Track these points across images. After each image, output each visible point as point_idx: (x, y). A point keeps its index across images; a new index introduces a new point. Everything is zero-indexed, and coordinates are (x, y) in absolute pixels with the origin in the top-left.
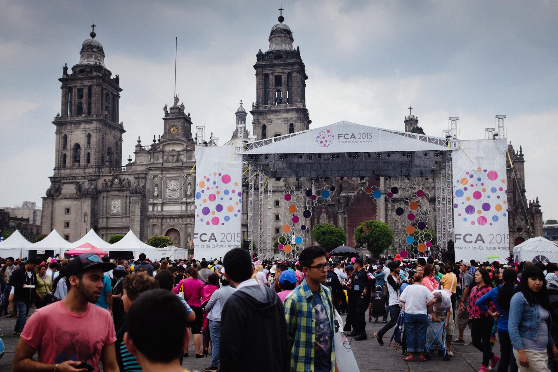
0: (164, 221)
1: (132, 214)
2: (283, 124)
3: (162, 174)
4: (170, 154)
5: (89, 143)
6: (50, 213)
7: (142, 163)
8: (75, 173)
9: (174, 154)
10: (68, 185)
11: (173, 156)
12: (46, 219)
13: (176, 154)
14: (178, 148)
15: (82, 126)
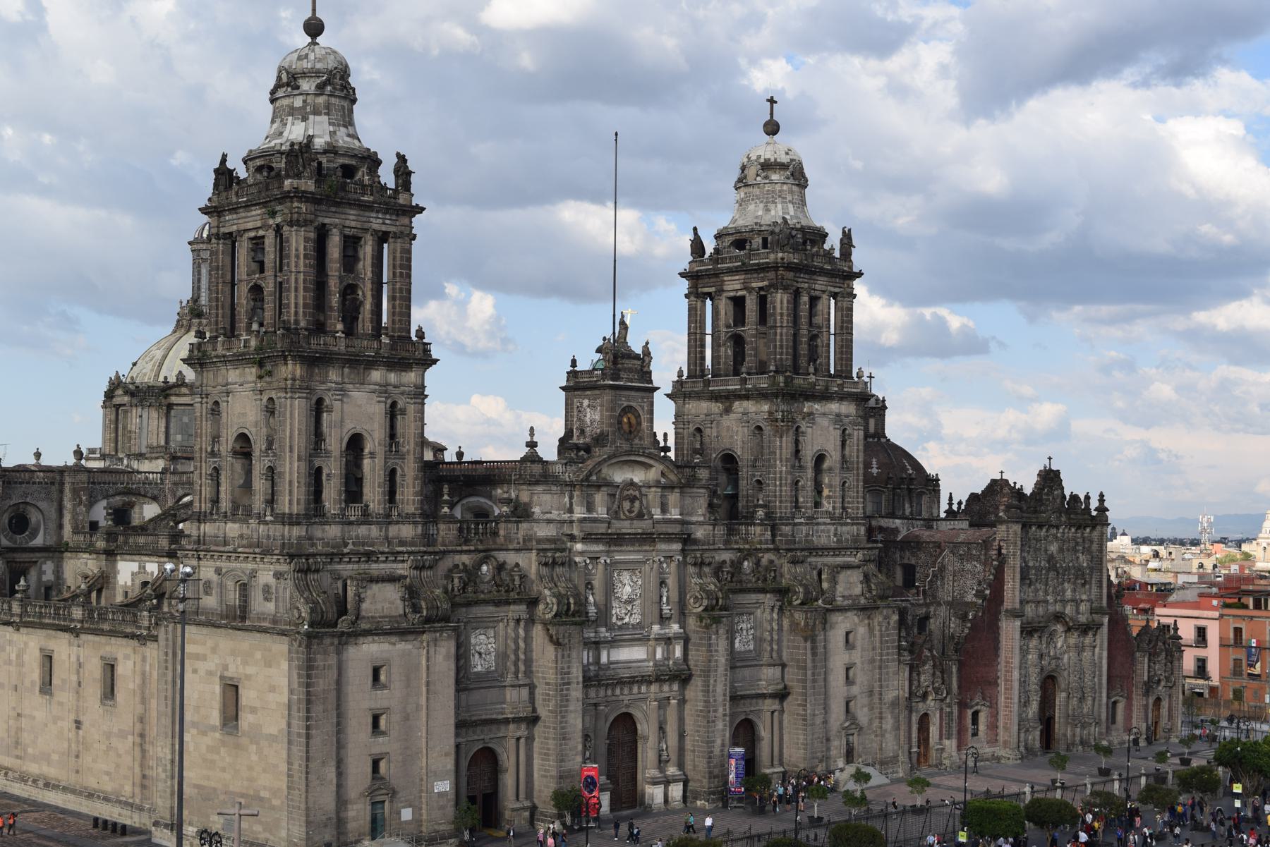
0: (609, 692)
1: (563, 679)
2: (831, 428)
3: (608, 553)
4: (626, 493)
5: (392, 436)
6: (333, 687)
7: (548, 516)
8: (357, 537)
9: (634, 493)
10: (380, 585)
11: (633, 500)
12: (321, 708)
13: (637, 493)
14: (638, 476)
15: (376, 375)
